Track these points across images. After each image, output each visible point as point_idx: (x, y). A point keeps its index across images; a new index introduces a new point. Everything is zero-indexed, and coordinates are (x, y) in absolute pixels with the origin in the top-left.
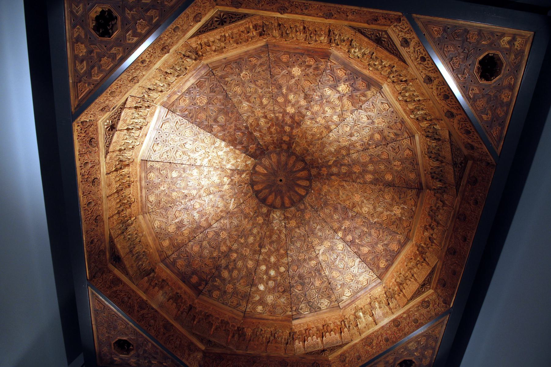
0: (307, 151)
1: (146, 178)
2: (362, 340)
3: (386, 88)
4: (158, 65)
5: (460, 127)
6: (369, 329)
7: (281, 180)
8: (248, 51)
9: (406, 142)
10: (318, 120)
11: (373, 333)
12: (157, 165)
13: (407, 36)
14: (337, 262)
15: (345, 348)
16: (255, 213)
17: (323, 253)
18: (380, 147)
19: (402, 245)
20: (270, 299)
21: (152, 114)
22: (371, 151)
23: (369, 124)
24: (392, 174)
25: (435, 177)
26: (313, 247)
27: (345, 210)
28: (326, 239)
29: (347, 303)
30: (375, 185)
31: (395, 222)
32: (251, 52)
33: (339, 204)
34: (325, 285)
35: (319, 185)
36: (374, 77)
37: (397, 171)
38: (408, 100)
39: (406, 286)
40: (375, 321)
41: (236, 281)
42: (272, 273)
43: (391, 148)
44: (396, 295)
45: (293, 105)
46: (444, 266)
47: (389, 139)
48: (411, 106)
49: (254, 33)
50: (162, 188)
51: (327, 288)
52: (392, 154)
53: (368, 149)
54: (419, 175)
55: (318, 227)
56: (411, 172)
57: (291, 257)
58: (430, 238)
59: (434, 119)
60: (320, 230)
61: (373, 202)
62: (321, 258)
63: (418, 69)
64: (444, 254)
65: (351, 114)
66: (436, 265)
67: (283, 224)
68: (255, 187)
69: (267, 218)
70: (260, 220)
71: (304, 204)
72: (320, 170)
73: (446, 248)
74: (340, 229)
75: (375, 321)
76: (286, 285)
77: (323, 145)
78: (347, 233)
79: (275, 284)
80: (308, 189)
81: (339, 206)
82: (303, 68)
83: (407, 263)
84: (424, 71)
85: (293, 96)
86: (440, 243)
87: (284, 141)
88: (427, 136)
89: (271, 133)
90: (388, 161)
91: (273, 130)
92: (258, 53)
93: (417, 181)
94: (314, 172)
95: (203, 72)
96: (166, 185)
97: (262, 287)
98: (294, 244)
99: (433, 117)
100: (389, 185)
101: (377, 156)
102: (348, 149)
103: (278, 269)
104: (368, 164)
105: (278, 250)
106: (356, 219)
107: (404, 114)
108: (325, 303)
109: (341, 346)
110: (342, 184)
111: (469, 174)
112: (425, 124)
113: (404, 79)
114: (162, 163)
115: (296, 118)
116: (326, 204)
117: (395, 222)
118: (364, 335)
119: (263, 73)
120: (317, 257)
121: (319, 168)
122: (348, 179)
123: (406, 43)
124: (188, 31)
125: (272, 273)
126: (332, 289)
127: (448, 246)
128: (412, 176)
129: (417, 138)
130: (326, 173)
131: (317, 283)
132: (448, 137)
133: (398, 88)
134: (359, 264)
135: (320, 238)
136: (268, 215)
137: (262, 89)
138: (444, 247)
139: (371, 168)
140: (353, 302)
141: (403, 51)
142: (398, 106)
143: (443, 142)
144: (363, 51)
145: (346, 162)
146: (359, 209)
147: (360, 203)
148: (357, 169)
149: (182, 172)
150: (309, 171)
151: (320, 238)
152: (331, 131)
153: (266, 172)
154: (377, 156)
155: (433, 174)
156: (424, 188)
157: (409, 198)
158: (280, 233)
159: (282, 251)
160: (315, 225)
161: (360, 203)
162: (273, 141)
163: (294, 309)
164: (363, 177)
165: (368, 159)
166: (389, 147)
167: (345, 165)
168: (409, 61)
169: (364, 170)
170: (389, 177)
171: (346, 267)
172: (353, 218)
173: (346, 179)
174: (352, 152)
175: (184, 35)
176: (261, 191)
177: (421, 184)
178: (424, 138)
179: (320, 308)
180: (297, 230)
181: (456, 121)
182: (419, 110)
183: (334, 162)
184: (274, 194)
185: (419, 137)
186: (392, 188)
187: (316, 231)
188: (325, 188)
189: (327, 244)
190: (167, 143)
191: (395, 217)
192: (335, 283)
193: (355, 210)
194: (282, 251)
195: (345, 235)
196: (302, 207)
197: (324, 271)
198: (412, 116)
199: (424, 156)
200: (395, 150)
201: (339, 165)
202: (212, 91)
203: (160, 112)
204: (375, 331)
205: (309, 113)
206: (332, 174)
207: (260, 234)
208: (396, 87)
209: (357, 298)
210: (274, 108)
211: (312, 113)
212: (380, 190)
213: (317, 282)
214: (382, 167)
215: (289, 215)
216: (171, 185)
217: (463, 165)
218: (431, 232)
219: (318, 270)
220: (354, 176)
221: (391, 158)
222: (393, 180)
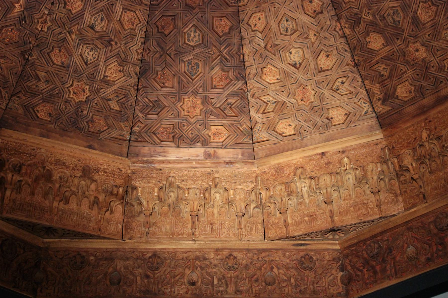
1: (412, 101)
4: (185, 245)
8: (42, 136)
12: (376, 89)
21: (279, 169)
32: (38, 130)
49: (10, 176)
50: (422, 53)
92: (27, 120)
95: (145, 150)
96: (411, 48)
114: (367, 82)
119: (42, 74)
124: (107, 251)
137: (64, 40)
149: (362, 25)
175: (117, 250)
190: (317, 103)
202: (157, 107)
203: (267, 156)
216: (406, 34)
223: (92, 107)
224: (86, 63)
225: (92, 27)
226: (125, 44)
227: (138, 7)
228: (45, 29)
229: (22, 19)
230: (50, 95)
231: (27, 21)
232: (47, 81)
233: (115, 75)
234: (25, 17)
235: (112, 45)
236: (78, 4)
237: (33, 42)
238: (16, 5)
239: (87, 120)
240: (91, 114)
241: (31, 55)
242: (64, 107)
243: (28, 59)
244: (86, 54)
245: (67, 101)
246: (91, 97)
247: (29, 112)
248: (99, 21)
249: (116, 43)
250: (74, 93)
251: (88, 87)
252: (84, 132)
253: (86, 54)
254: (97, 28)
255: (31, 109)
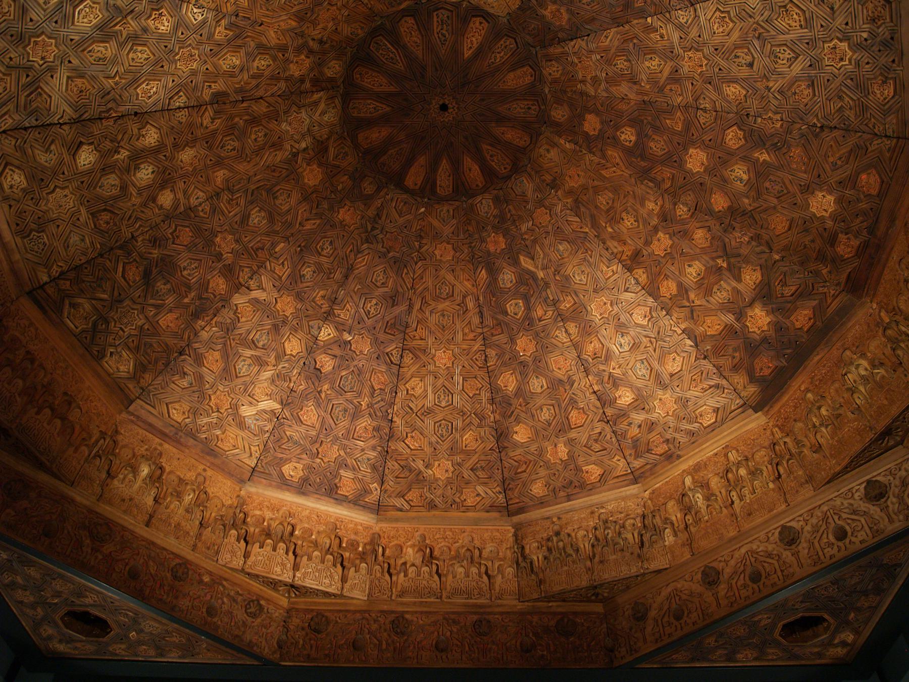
0: (554, 185)
2: (91, 511)
3: (756, 422)
5: (684, 597)
6: (125, 512)
7: (444, 108)
9: (620, 465)
10: (660, 234)
11: (124, 528)
13: (892, 502)
14: (248, 353)
15: (43, 477)
16: (321, 42)
17: (256, 300)
18: (598, 404)
19: (356, 501)
20: (62, 201)
22: (582, 383)
23: (658, 376)
24: (532, 440)
25: (550, 544)
26: (262, 265)
27: (398, 328)
28: (299, 297)
29: (152, 420)
30: (492, 401)
31: (410, 471)
33: (411, 307)
34: (171, 341)
35: (447, 230)
36: (785, 398)
37: (541, 452)
38: (730, 475)
39: (268, 548)
40: (151, 516)
41: (76, 62)
42: (145, 174)
43: (598, 430)
44: (233, 532)
45: (710, 171)
46: (358, 616)
47: (623, 426)
48: (715, 483)
51: (168, 349)
52: (582, 437)
53: (587, 372)
54: (542, 503)
55: (323, 260)
56: (547, 485)
57: (214, 210)
58: (405, 564)
59: (690, 533)
60: (319, 266)
61: (443, 404)
62: (239, 300)
63: (811, 512)
64: (385, 608)
65: (683, 332)
66: (352, 598)
67: (303, 145)
68: (410, 21)
69: (307, 85)
70: (299, 67)
71: (379, 190)
72: (496, 229)
73: (400, 609)
74: (340, 327)
75: (151, 516)
76: (124, 228)
77: (578, 242)
78: (337, 352)
79: (115, 198)
80: (427, 192)
81: (403, 308)
82: (829, 224)
83: (324, 531)
84: (808, 528)
85: (745, 177)
86: (402, 594)
87: (581, 118)
88: (644, 516)
89: (612, 81)
90: (564, 428)
91: (624, 89)
93: (527, 500)
94: (485, 205)
97: (86, 158)
98: (252, 203)
99: (693, 529)
100: (502, 436)
101: (571, 399)
102: (578, 313)
103: (162, 187)
104: (546, 377)
105: (219, 163)
106: (383, 368)
107: (691, 463)
108: (121, 364)
109: (41, 466)
110: (471, 304)
111: (575, 614)
112: (674, 513)
113: (782, 471)
115: (667, 172)
116: (399, 265)
117: (410, 471)
118: (106, 509)
120: (237, 287)
121: (502, 224)
122: (489, 322)
123: (876, 493)
125: (145, 174)
126: (167, 365)
127: (407, 612)
128: (538, 489)
129: (633, 489)
130: (492, 249)
131: (167, 320)
132: (654, 566)
133: (762, 456)
134: (265, 411)
135: (296, 277)
136: (318, 83)
137: (780, 92)
138: (402, 604)
139: (537, 384)
140: (163, 436)
141: (856, 484)
142: (709, 449)
143: (639, 556)
144: (862, 388)
145: (540, 312)
146: (413, 369)
147: (431, 368)
148: (525, 346)
150: (485, 190)
151: (296, 277)
152: (630, 269)
153: (467, 54)
154: (571, 399)
155: (555, 539)
156: (516, 519)
157: (480, 489)
158: (273, 145)
159: (220, 175)
160: (328, 250)
161: (431, 368)
162: (583, 82)
163: (65, 285)
164: (504, 364)
165: (560, 374)
166: (599, 427)
167: (528, 308)
168: (830, 493)
169: (523, 364)
170: (521, 434)
171: (244, 384)
172: (381, 356)
173: (486, 314)
174: (572, 328)
176: (397, 41)
177: (521, 510)
178: (640, 511)
179: (104, 356)
180: (295, 197)
181: (697, 588)
182: (707, 498)
183: (529, 272)
184: (392, 89)
185: (636, 496)
186: (491, 443)
187: (313, 259)
188: (444, 253)
189: (287, 306)
191: (422, 468)
192: (188, 369)
193: (408, 359)
194: (220, 175)
195: (326, 347)
196: (368, 188)
197: (209, 323)
198: (688, 481)
199: (592, 513)
200: (596, 441)
201: (522, 289)
204: (132, 533)
205: (682, 211)
206: (493, 272)
207: (254, 82)
208: (763, 453)
209: (178, 442)
210: (705, 110)
211: (683, 222)
212: (481, 417)
213: (170, 317)
214: (545, 415)
215: (332, 152)
217: (593, 598)
218: (418, 562)
219: (203, 307)
220: (502, 339)
221: (573, 434)
222: (516, 445)
223: (852, 28)
224: (796, 58)
225: (751, 65)
226: (751, 17)
227: (702, 18)
228: (778, 117)
229: (776, 148)
230: (857, 89)
231: (776, 141)
232: (840, 98)
233: (795, 16)
234: (772, 145)
235: (760, 34)
236: (734, 90)
237: (798, 126)
238: (761, 160)
239: (876, 29)
240: (865, 26)
241: (815, 125)
242: (867, 66)
243: (822, 127)
244: (785, 62)
245: (858, 64)
246: (838, 35)
247: (890, 109)
248: (740, 60)
249: (755, 30)
250: (841, 59)
251: (826, 45)
252: (896, 26)
253: (785, 62)
254: (749, 59)
255: (886, 107)
